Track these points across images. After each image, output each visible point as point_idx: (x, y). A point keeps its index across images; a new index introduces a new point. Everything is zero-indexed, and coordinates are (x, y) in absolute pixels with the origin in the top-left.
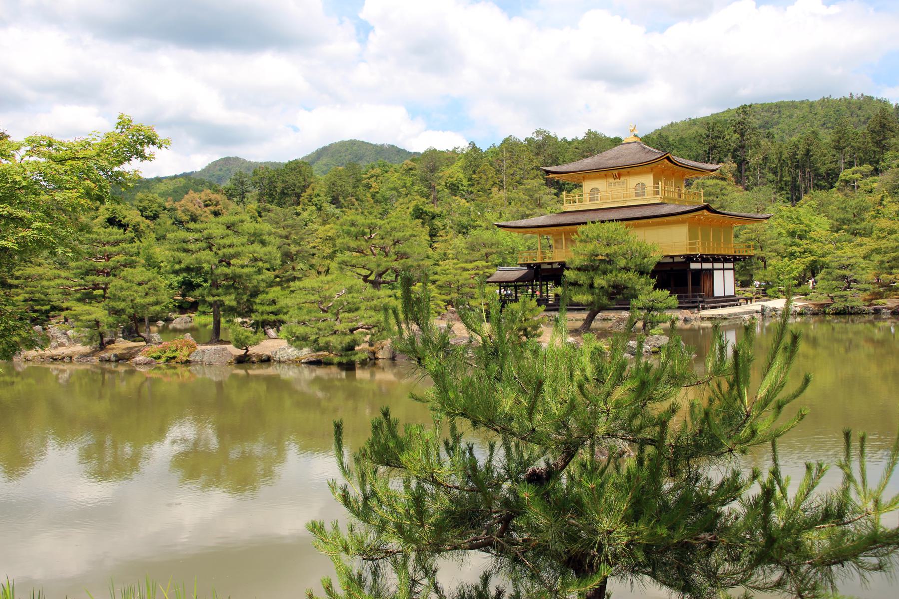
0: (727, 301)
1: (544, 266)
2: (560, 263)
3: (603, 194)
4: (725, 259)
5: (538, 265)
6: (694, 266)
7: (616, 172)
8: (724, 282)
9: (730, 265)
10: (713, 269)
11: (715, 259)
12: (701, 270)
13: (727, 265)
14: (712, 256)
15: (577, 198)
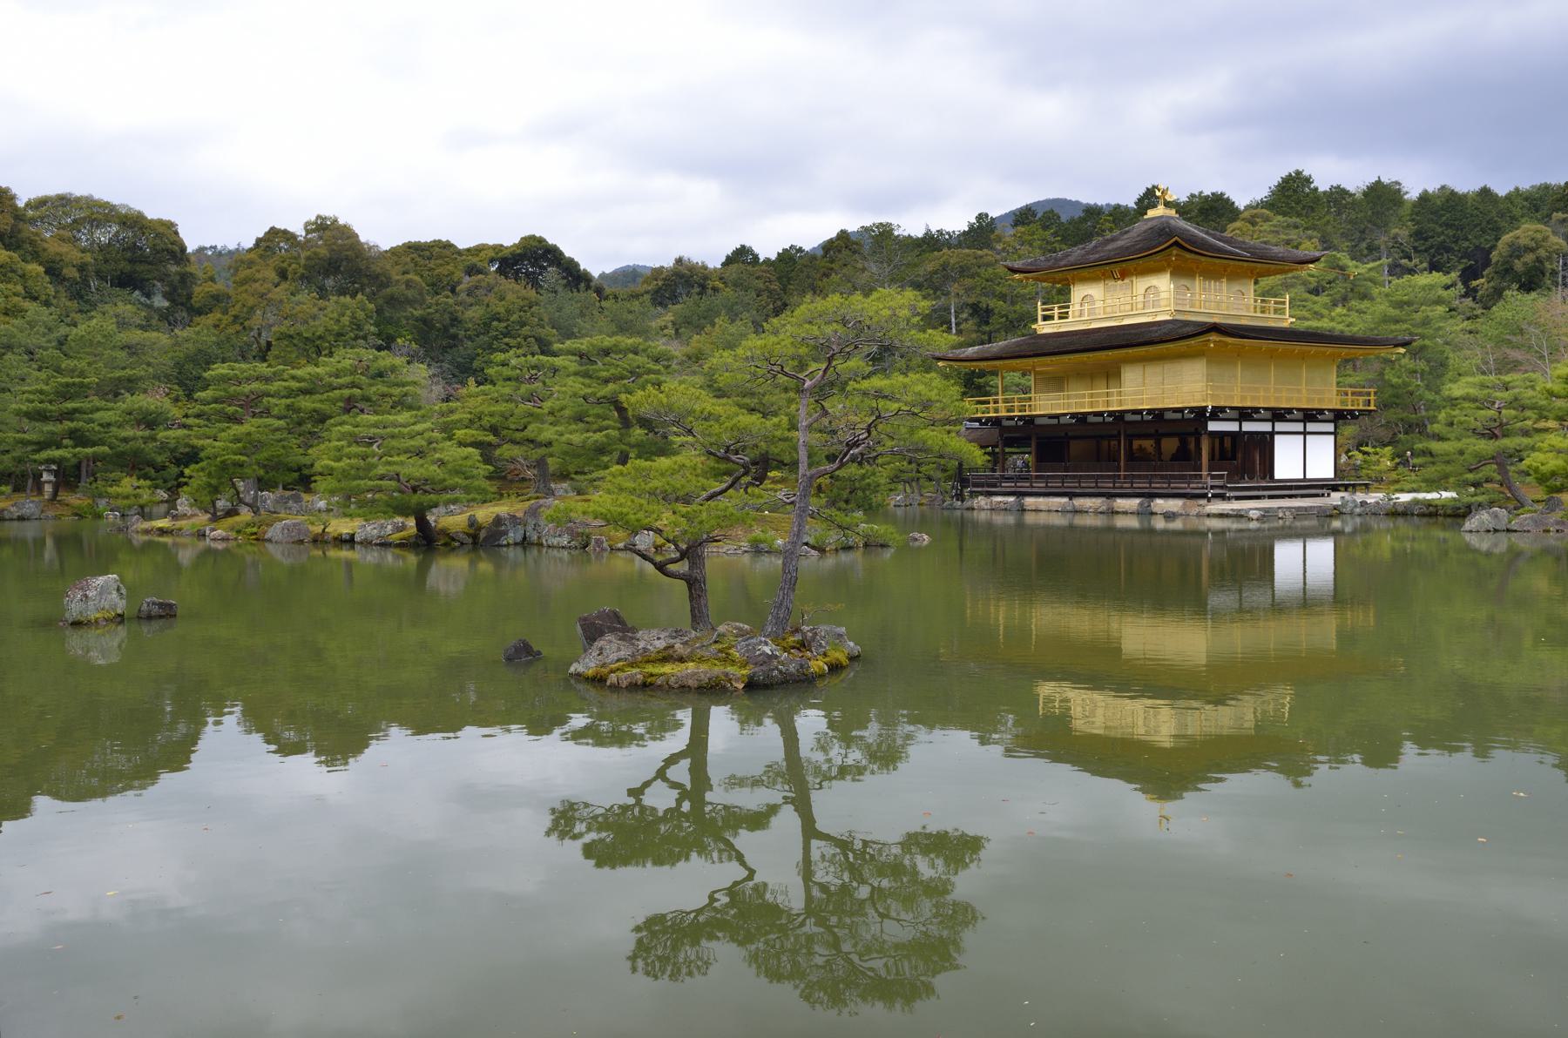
0: (1290, 488)
1: (1005, 423)
2: (1021, 418)
3: (1099, 304)
4: (1309, 416)
5: (997, 422)
6: (1213, 426)
7: (1117, 269)
8: (1303, 457)
9: (1330, 427)
10: (1272, 434)
11: (1278, 415)
12: (1240, 434)
13: (1311, 427)
14: (1256, 410)
15: (1056, 311)
